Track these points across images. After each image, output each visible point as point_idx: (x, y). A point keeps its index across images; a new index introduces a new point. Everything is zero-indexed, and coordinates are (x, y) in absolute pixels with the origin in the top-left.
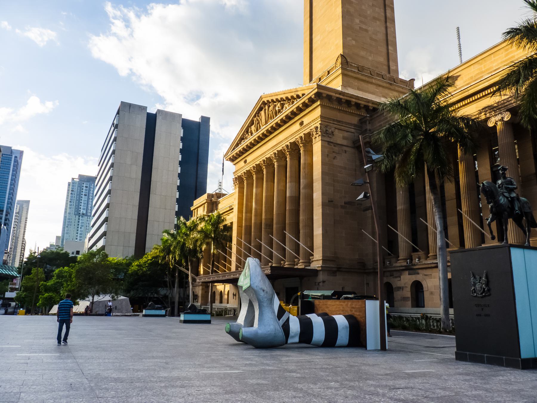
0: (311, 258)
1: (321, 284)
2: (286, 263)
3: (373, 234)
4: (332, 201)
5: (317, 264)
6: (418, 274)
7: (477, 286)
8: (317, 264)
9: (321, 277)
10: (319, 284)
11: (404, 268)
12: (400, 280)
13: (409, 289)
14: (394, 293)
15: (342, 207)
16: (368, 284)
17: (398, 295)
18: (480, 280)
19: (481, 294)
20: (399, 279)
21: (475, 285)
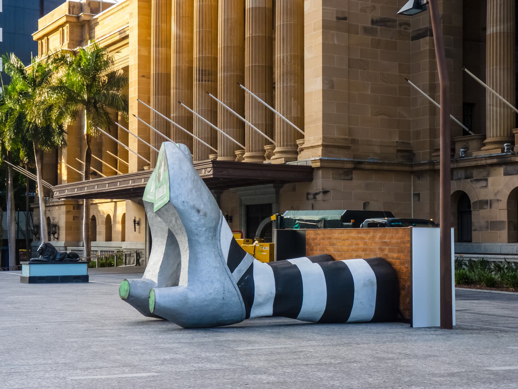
0: (298, 142)
1: (320, 197)
2: (247, 154)
3: (432, 89)
4: (345, 19)
5: (310, 156)
8: (310, 156)
9: (320, 182)
10: (315, 198)
11: (495, 161)
12: (486, 186)
13: (503, 204)
14: (474, 213)
15: (366, 30)
16: (417, 195)
17: (479, 217)
20: (483, 183)
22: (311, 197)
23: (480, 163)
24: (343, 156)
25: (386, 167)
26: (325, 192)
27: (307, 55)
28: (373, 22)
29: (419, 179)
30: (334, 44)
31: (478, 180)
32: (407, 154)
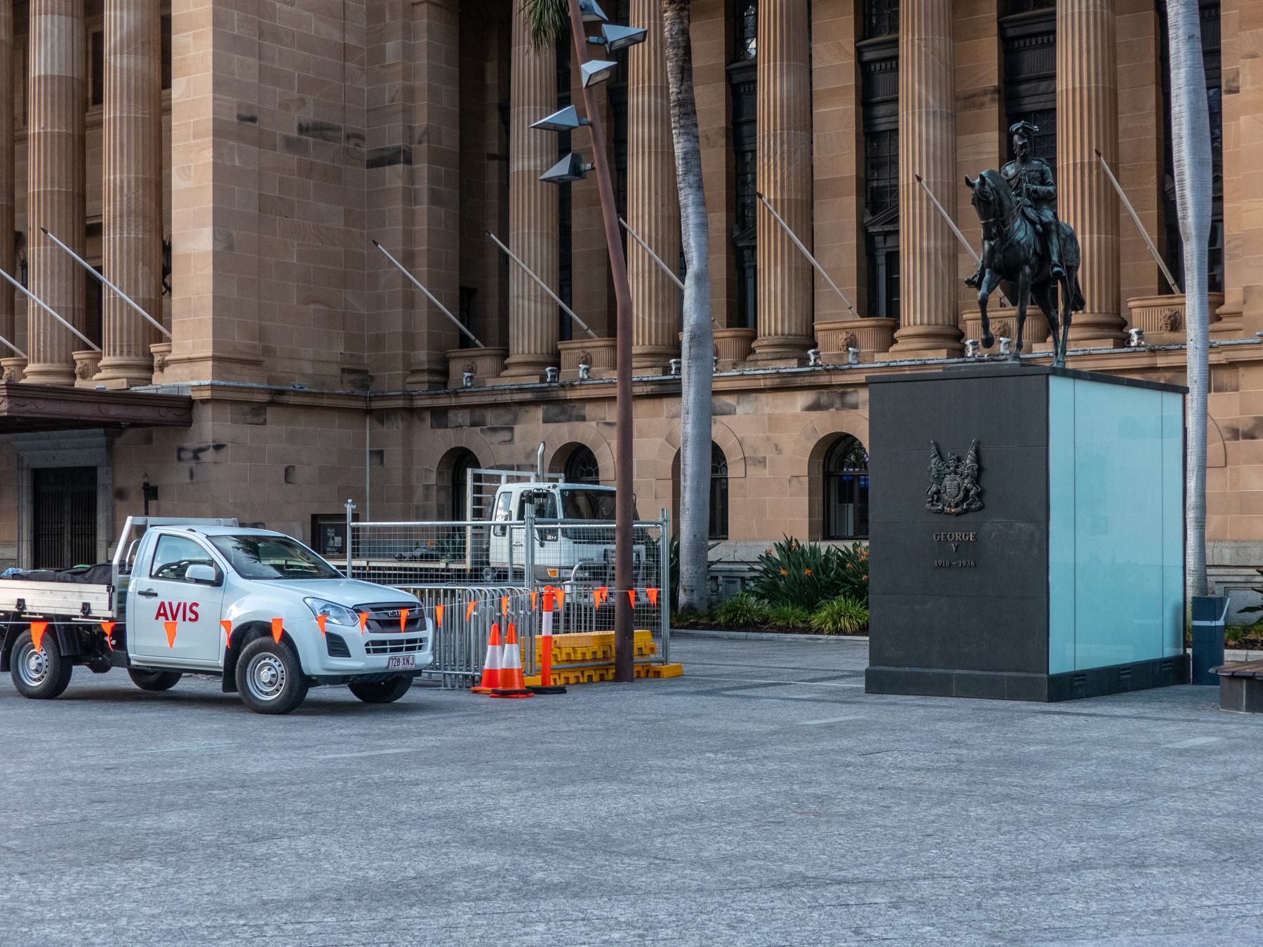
0: (154, 348)
1: (208, 456)
2: (31, 367)
3: (409, 259)
4: (253, 119)
6: (583, 418)
7: (947, 481)
9: (208, 426)
10: (196, 457)
11: (528, 396)
12: (511, 441)
15: (289, 143)
16: (378, 454)
18: (957, 467)
19: (957, 505)
20: (505, 436)
21: (940, 478)
22: (189, 455)
23: (500, 399)
24: (249, 379)
25: (325, 402)
26: (218, 447)
27: (178, 183)
28: (302, 129)
29: (383, 424)
30: (233, 166)
31: (494, 430)
32: (360, 376)
